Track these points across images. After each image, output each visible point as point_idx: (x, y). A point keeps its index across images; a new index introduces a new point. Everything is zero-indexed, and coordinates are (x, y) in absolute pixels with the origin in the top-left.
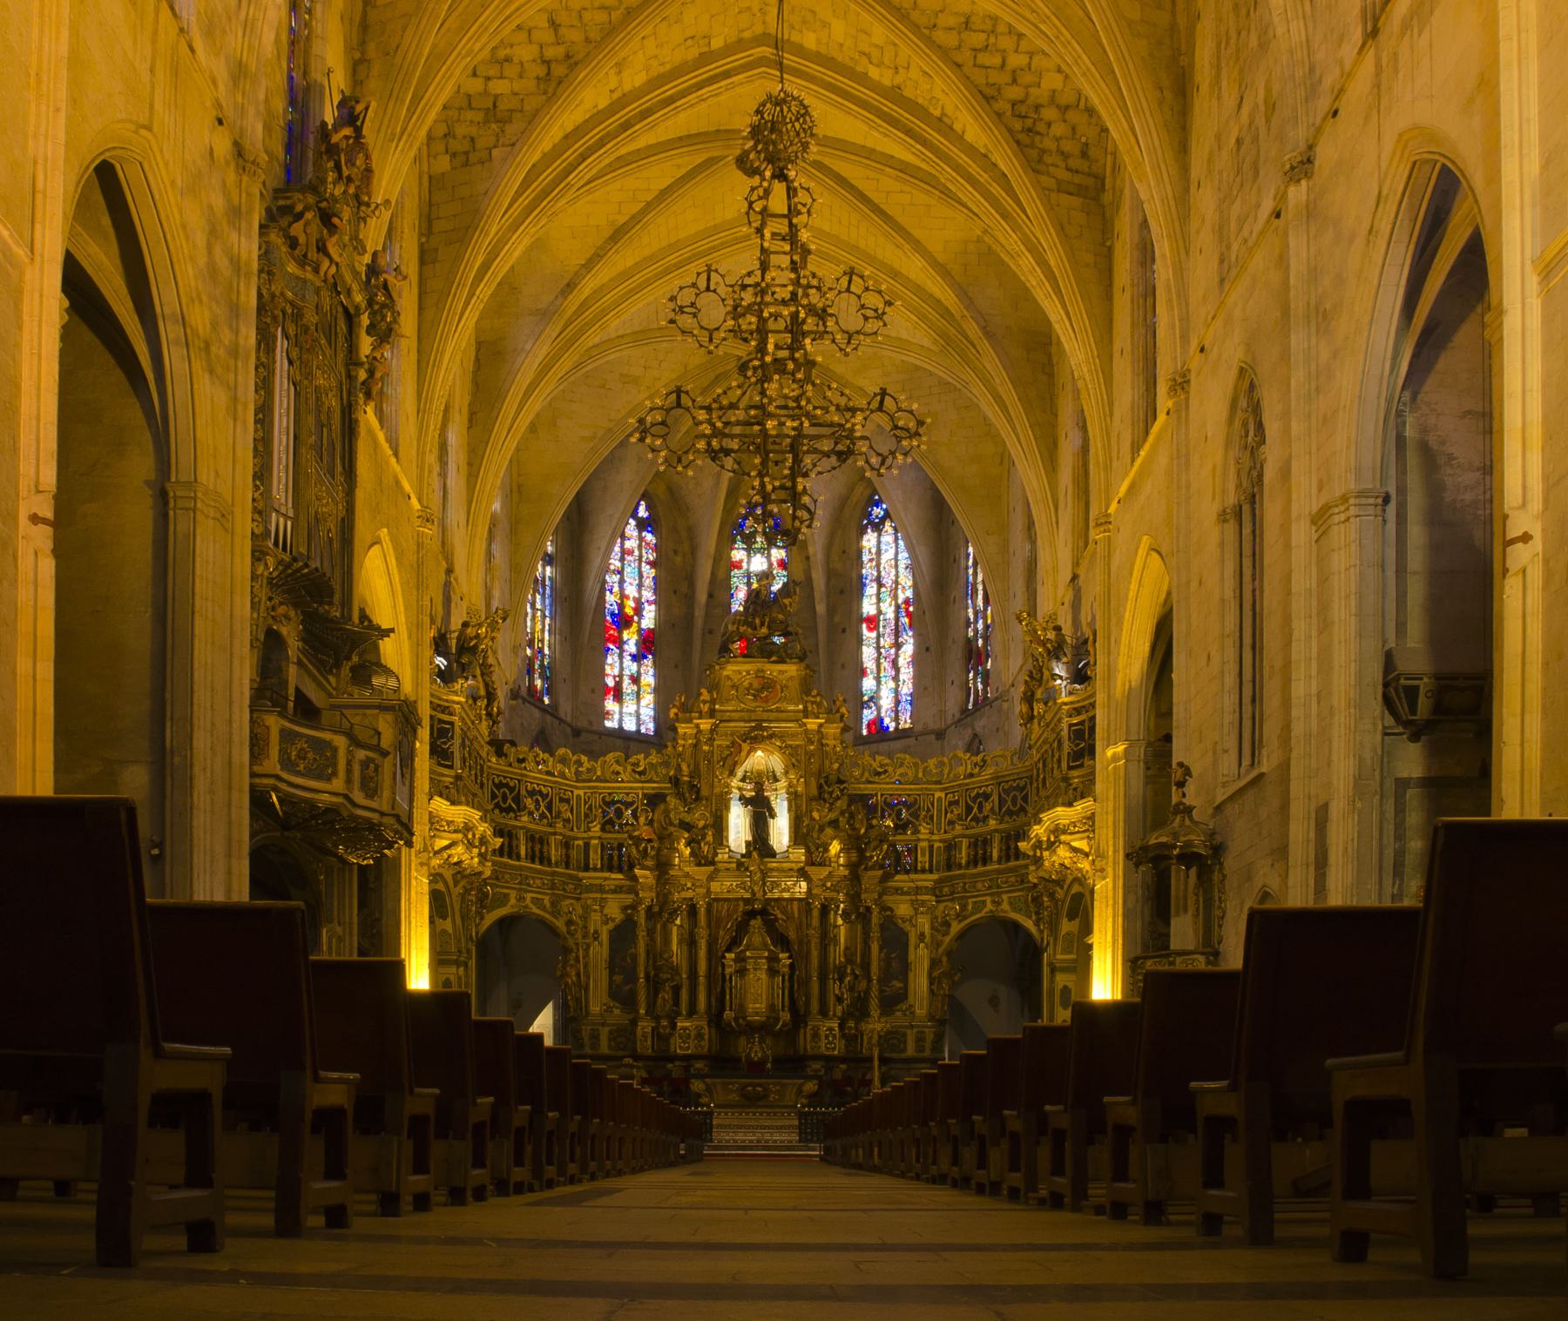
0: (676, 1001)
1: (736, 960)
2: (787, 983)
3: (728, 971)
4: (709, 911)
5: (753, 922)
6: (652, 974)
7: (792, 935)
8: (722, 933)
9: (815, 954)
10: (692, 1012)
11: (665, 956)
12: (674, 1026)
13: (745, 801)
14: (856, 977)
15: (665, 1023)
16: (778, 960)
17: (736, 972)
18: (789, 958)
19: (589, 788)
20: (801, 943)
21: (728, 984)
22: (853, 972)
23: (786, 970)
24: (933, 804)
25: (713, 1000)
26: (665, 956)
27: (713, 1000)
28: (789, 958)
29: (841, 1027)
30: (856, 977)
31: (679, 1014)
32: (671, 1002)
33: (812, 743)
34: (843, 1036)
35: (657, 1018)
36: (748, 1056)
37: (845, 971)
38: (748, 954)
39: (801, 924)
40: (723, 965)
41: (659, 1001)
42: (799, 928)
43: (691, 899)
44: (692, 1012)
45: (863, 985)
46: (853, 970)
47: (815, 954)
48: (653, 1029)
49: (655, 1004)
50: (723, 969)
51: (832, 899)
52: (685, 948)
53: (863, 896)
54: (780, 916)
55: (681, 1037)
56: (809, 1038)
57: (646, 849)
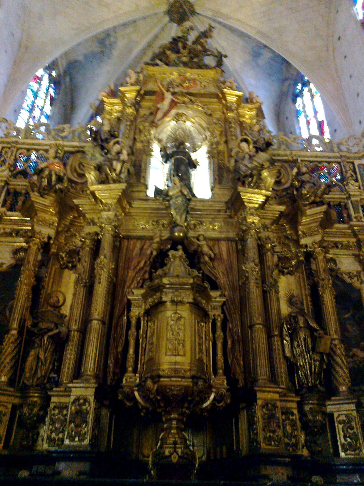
0: (58, 371)
1: (145, 297)
2: (219, 333)
3: (135, 312)
4: (117, 249)
5: (171, 253)
6: (29, 323)
7: (222, 279)
8: (131, 274)
9: (255, 292)
10: (77, 374)
11: (52, 301)
12: (47, 400)
13: (166, 157)
14: (312, 330)
15: (35, 397)
16: (209, 298)
17: (148, 313)
18: (220, 296)
19: (9, 143)
20: (233, 288)
21: (133, 330)
22: (308, 327)
23: (218, 312)
24: (354, 171)
25: (111, 363)
26: (52, 301)
27: (111, 363)
28: (220, 296)
29: (300, 405)
30: (312, 330)
31: (57, 384)
32: (48, 365)
33: (232, 111)
34: (305, 426)
35: (24, 391)
36: (159, 455)
37: (297, 322)
38: (165, 281)
39: (231, 268)
40: (129, 302)
41: (30, 359)
42: (229, 270)
43: (97, 234)
44: (77, 374)
45: (324, 346)
46: (306, 321)
47: (255, 292)
48: (15, 408)
49: (24, 361)
50: (129, 311)
51: (268, 238)
52: (82, 292)
53: (303, 241)
54: (206, 249)
55: (53, 422)
56: (260, 425)
57: (50, 175)
